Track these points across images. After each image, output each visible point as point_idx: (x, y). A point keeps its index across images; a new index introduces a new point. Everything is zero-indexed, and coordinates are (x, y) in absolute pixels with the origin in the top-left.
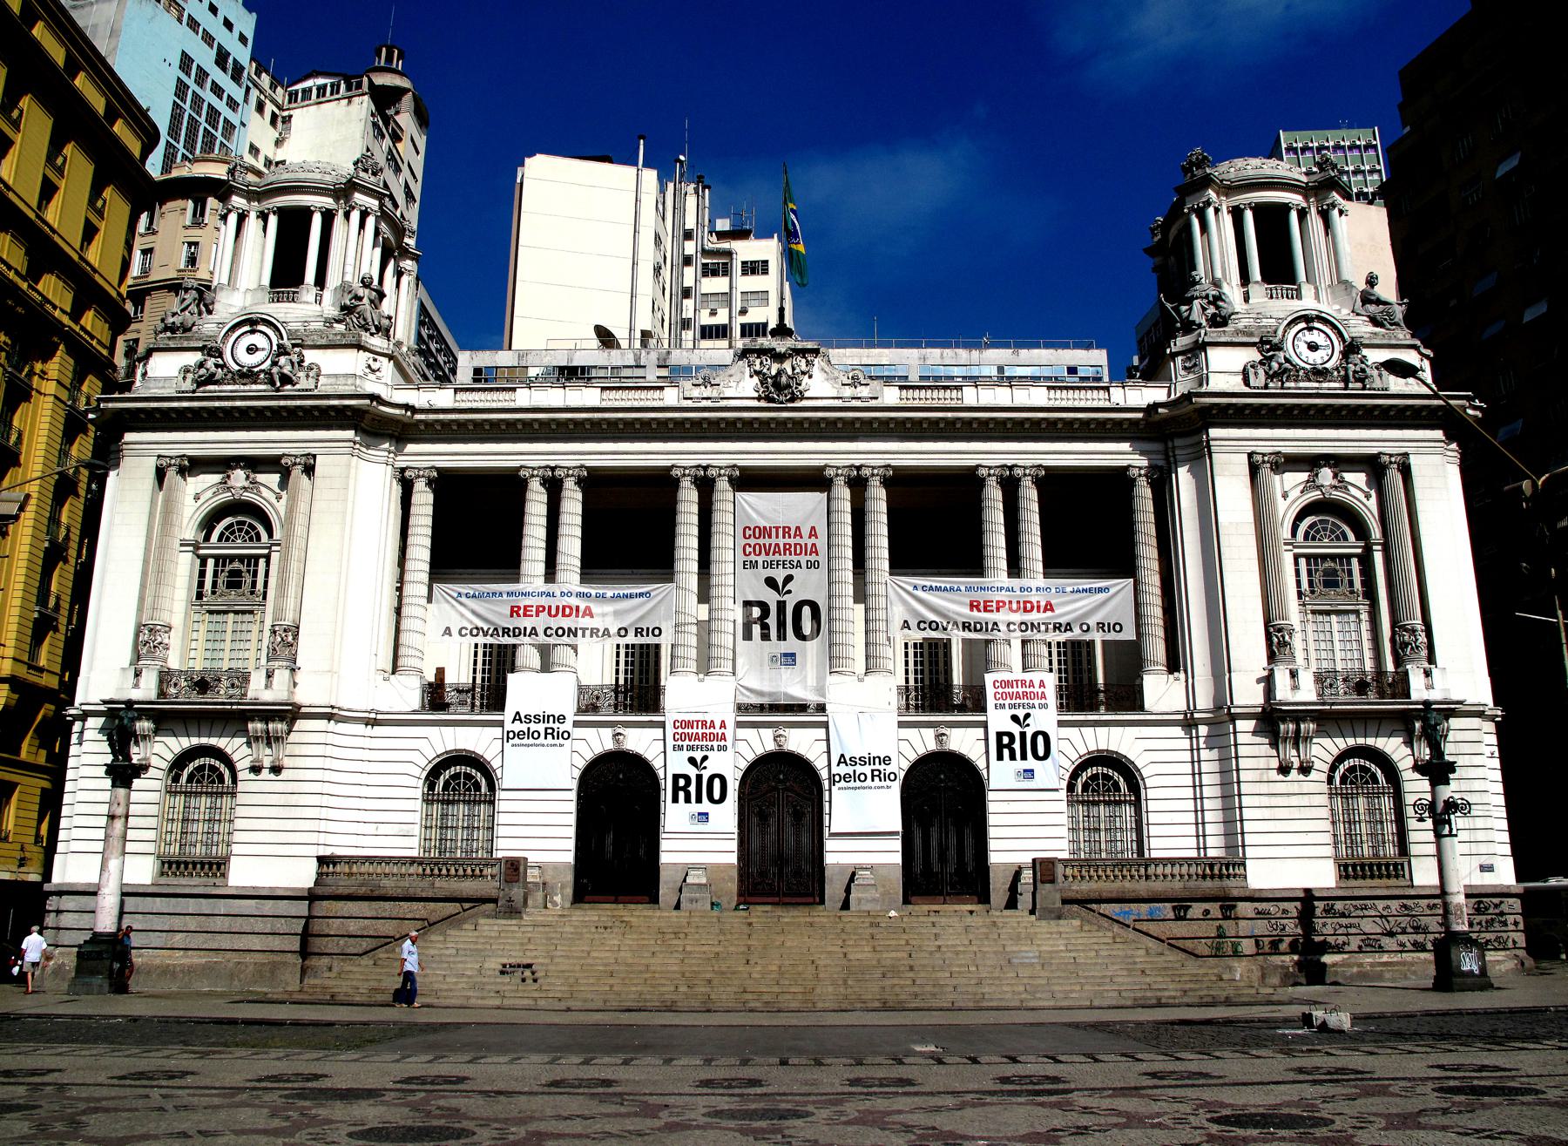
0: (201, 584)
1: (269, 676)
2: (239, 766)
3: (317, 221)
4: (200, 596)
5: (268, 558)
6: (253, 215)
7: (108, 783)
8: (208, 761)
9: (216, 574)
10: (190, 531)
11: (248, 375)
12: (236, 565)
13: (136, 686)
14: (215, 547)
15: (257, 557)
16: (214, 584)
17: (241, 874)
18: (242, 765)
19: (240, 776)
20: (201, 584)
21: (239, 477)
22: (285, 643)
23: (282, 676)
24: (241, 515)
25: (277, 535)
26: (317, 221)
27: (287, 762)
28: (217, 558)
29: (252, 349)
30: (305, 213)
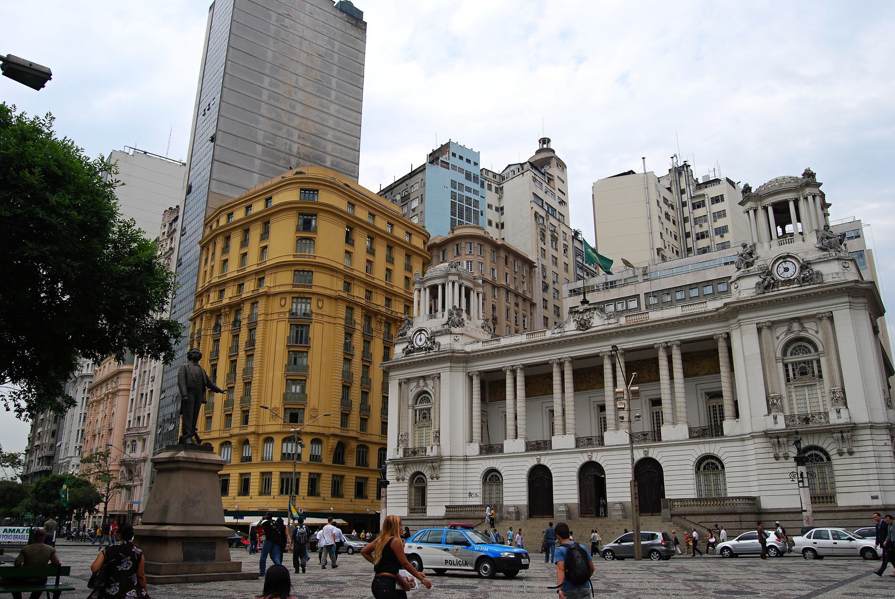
0: (788, 375)
1: (838, 412)
2: (831, 453)
4: (788, 380)
5: (818, 361)
6: (760, 208)
7: (795, 464)
8: (814, 452)
9: (793, 370)
10: (779, 354)
11: (789, 282)
12: (803, 365)
13: (776, 423)
14: (790, 359)
15: (812, 361)
16: (794, 375)
17: (842, 501)
18: (833, 452)
19: (833, 457)
20: (788, 375)
21: (796, 326)
22: (840, 398)
23: (844, 412)
24: (799, 343)
25: (821, 349)
27: (855, 449)
28: (792, 364)
29: (786, 270)
30: (786, 203)
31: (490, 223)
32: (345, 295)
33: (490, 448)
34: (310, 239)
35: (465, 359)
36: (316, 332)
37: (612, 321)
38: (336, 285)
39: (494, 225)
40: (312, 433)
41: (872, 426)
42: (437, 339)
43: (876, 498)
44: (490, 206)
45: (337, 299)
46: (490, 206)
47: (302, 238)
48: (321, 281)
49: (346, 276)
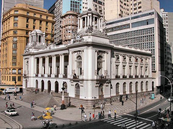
3: (86, 18)
7: (62, 89)
26: (86, 18)
31: (83, 8)
32: (26, 35)
33: (37, 76)
34: (17, 23)
35: (33, 54)
36: (18, 45)
37: (54, 47)
38: (24, 33)
39: (85, 8)
40: (18, 68)
41: (87, 80)
42: (30, 49)
43: (85, 97)
44: (84, 3)
45: (25, 37)
46: (84, 3)
47: (15, 23)
48: (19, 33)
49: (26, 30)
